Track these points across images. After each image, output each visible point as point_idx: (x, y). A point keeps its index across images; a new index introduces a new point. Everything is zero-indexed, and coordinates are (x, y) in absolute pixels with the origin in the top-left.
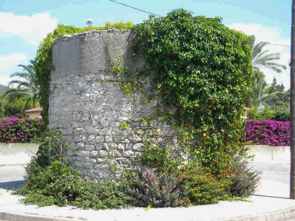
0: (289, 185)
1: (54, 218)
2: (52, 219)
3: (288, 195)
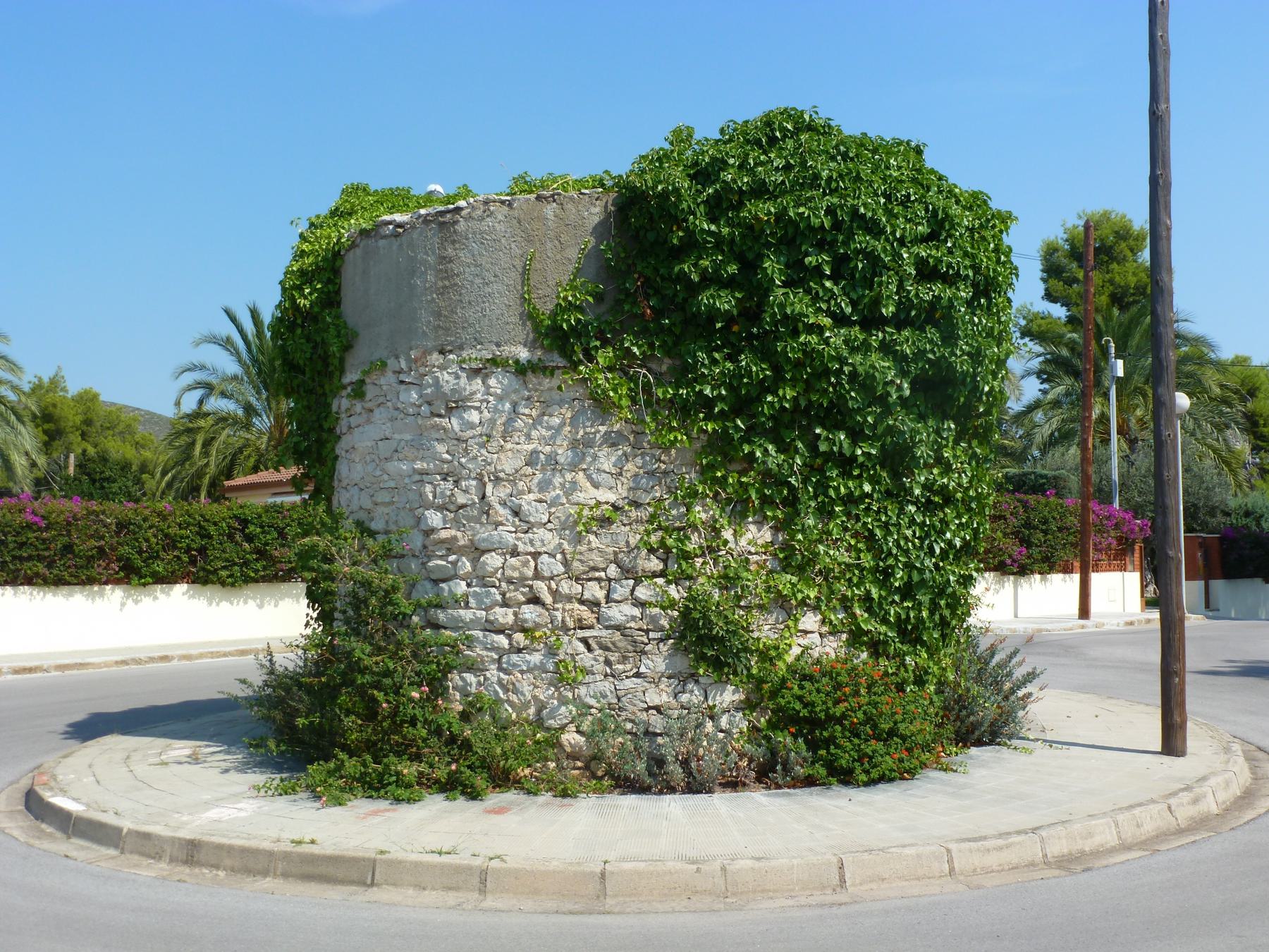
0: (1159, 711)
1: (379, 856)
2: (375, 861)
3: (1157, 744)
